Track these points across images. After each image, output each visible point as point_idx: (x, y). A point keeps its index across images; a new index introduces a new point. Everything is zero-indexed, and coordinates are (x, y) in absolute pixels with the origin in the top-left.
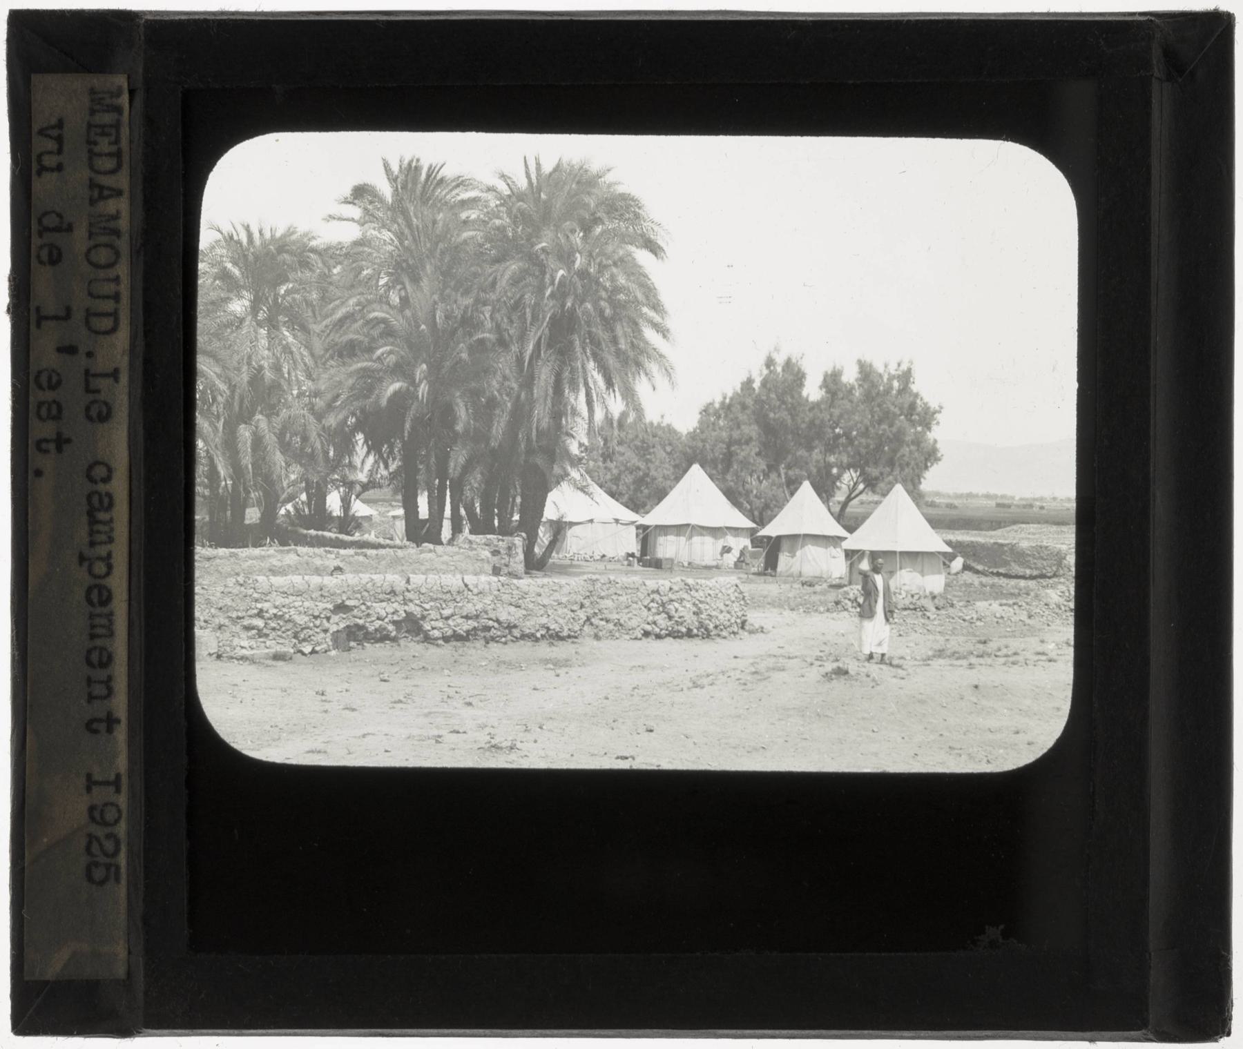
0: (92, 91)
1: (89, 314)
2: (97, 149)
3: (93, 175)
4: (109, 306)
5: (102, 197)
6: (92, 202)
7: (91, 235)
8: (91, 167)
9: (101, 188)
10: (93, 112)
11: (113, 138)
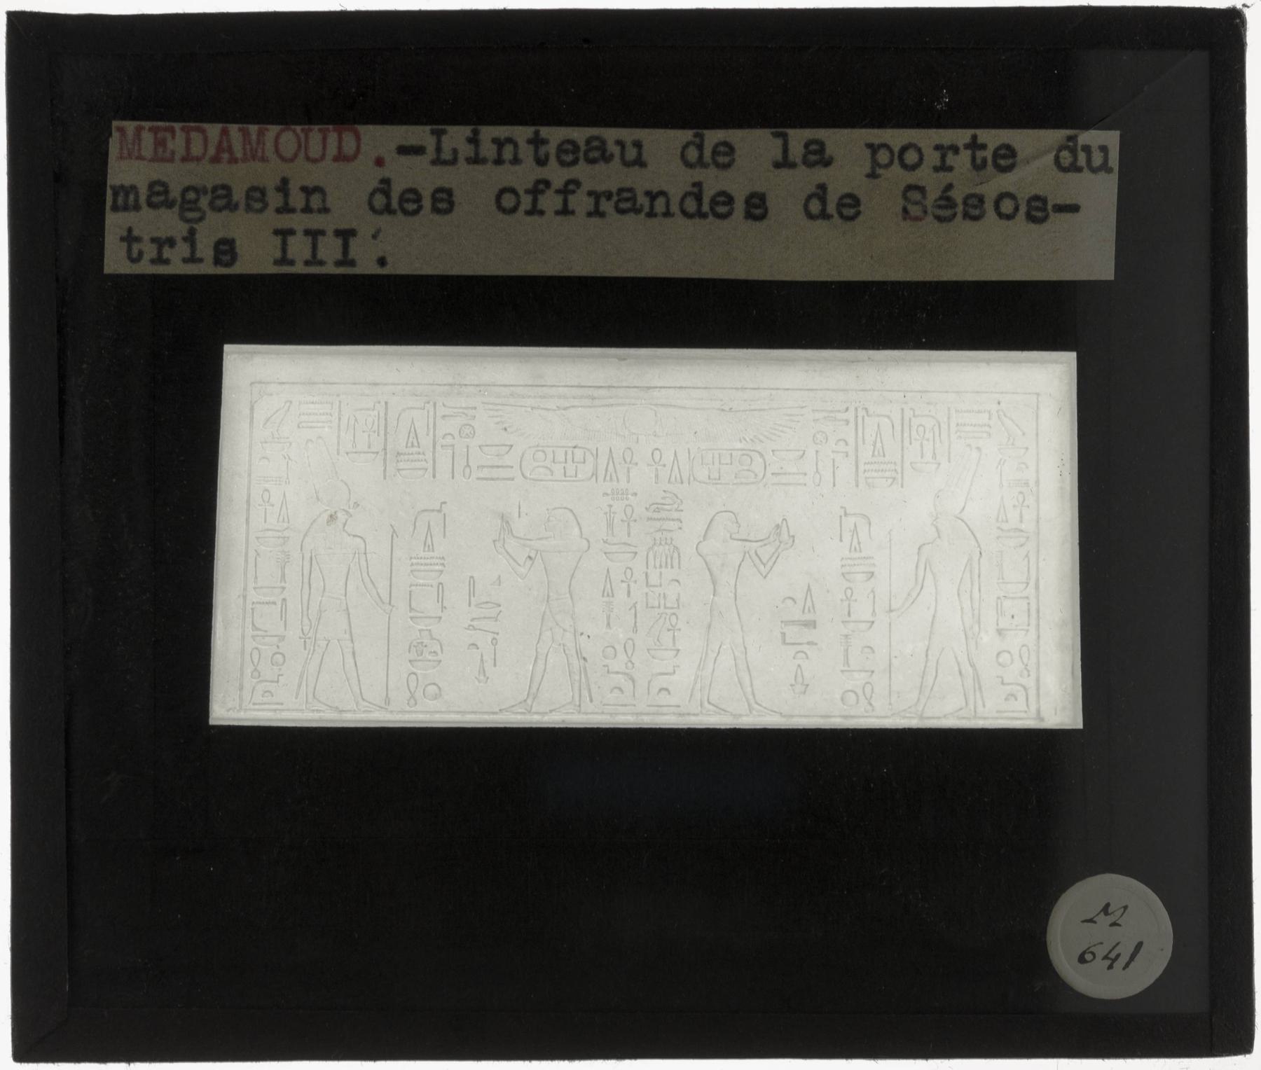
0: (121, 158)
1: (340, 157)
2: (181, 152)
3: (207, 158)
4: (333, 138)
5: (230, 150)
7: (264, 159)
8: (198, 159)
9: (219, 149)
10: (140, 158)
11: (168, 135)
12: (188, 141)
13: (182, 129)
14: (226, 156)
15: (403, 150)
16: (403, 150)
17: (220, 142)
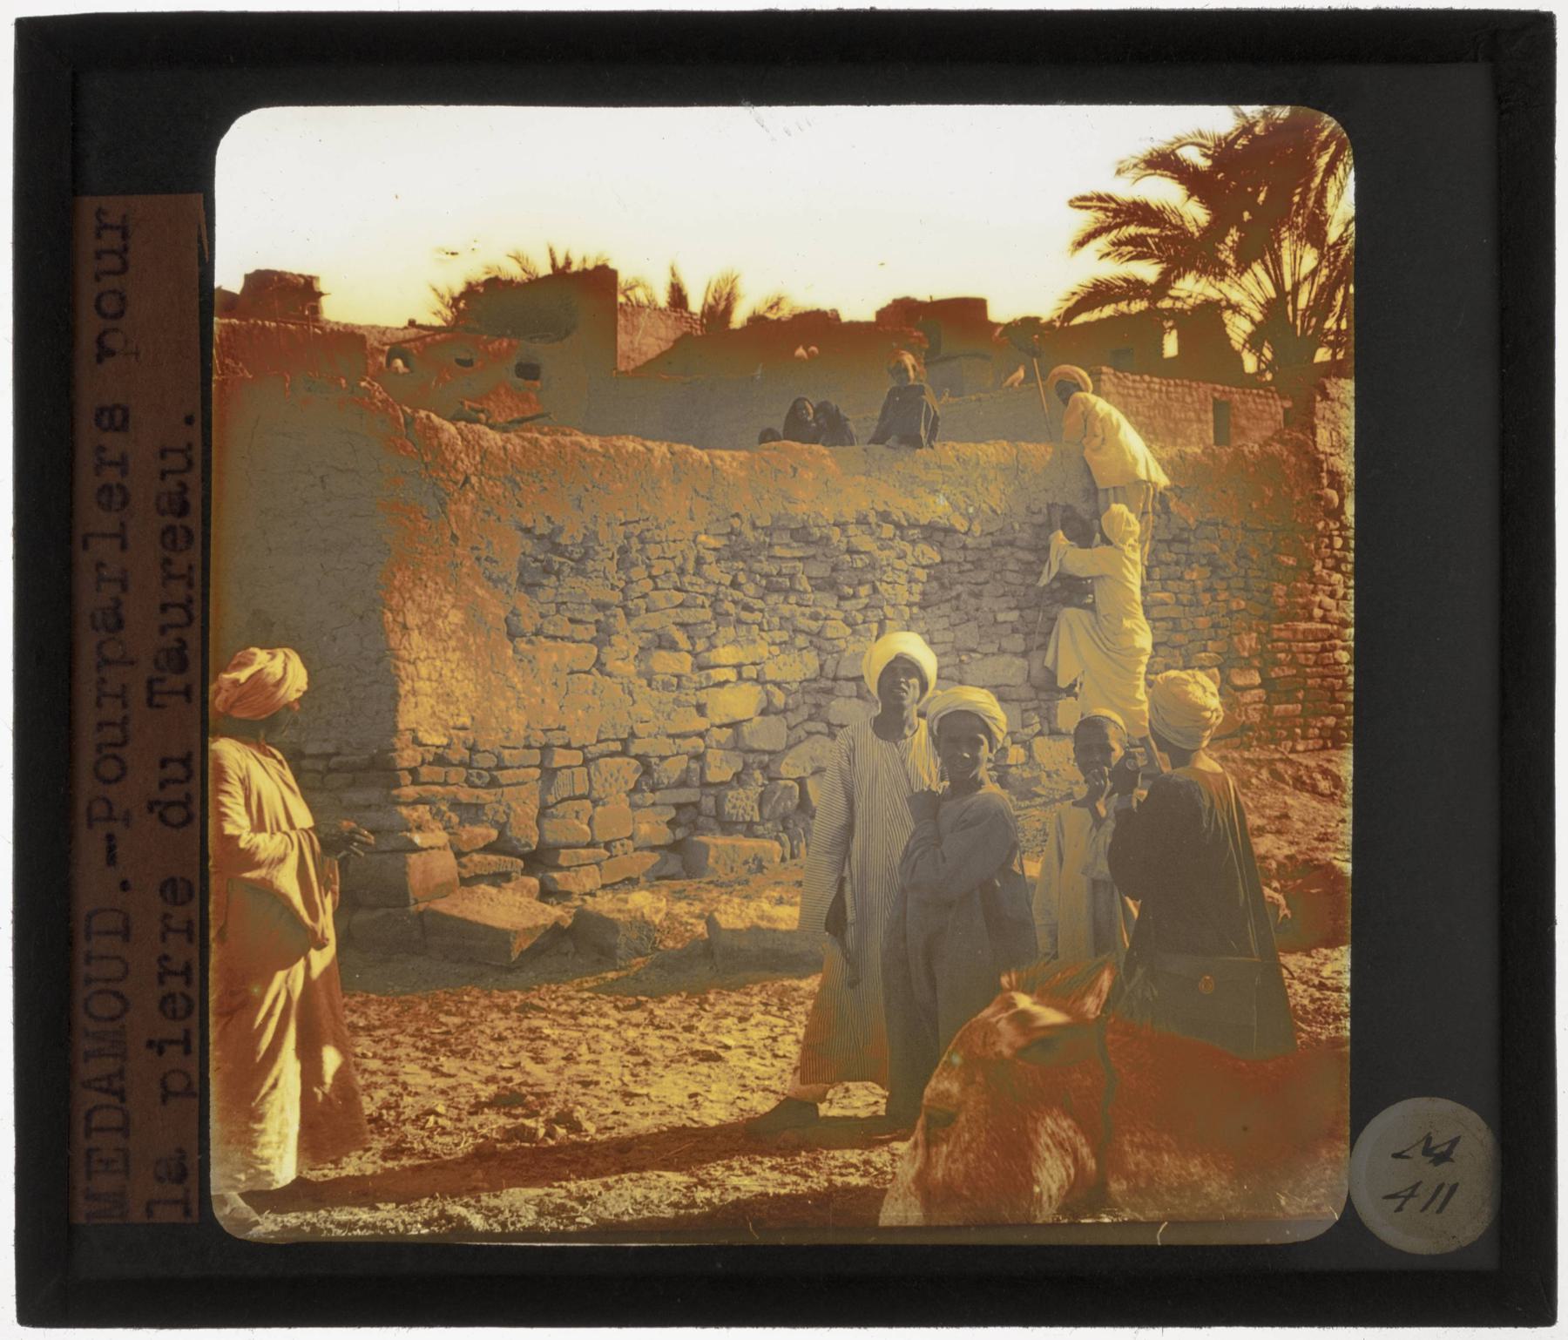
5: (109, 1077)
6: (121, 1074)
12: (100, 1129)
13: (88, 1134)
14: (117, 1084)
15: (111, 859)
16: (111, 859)
17: (100, 1090)
